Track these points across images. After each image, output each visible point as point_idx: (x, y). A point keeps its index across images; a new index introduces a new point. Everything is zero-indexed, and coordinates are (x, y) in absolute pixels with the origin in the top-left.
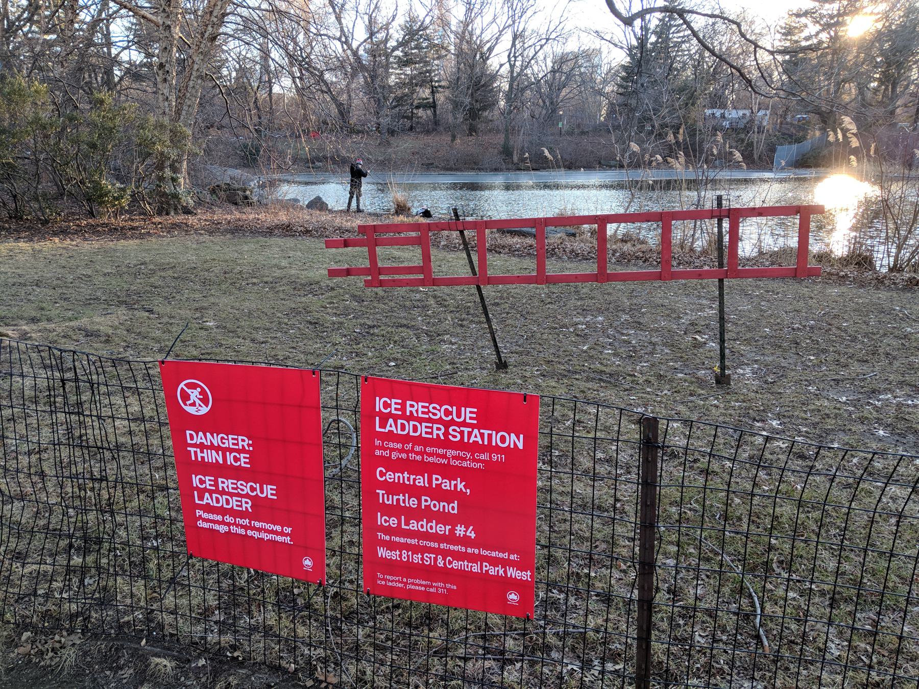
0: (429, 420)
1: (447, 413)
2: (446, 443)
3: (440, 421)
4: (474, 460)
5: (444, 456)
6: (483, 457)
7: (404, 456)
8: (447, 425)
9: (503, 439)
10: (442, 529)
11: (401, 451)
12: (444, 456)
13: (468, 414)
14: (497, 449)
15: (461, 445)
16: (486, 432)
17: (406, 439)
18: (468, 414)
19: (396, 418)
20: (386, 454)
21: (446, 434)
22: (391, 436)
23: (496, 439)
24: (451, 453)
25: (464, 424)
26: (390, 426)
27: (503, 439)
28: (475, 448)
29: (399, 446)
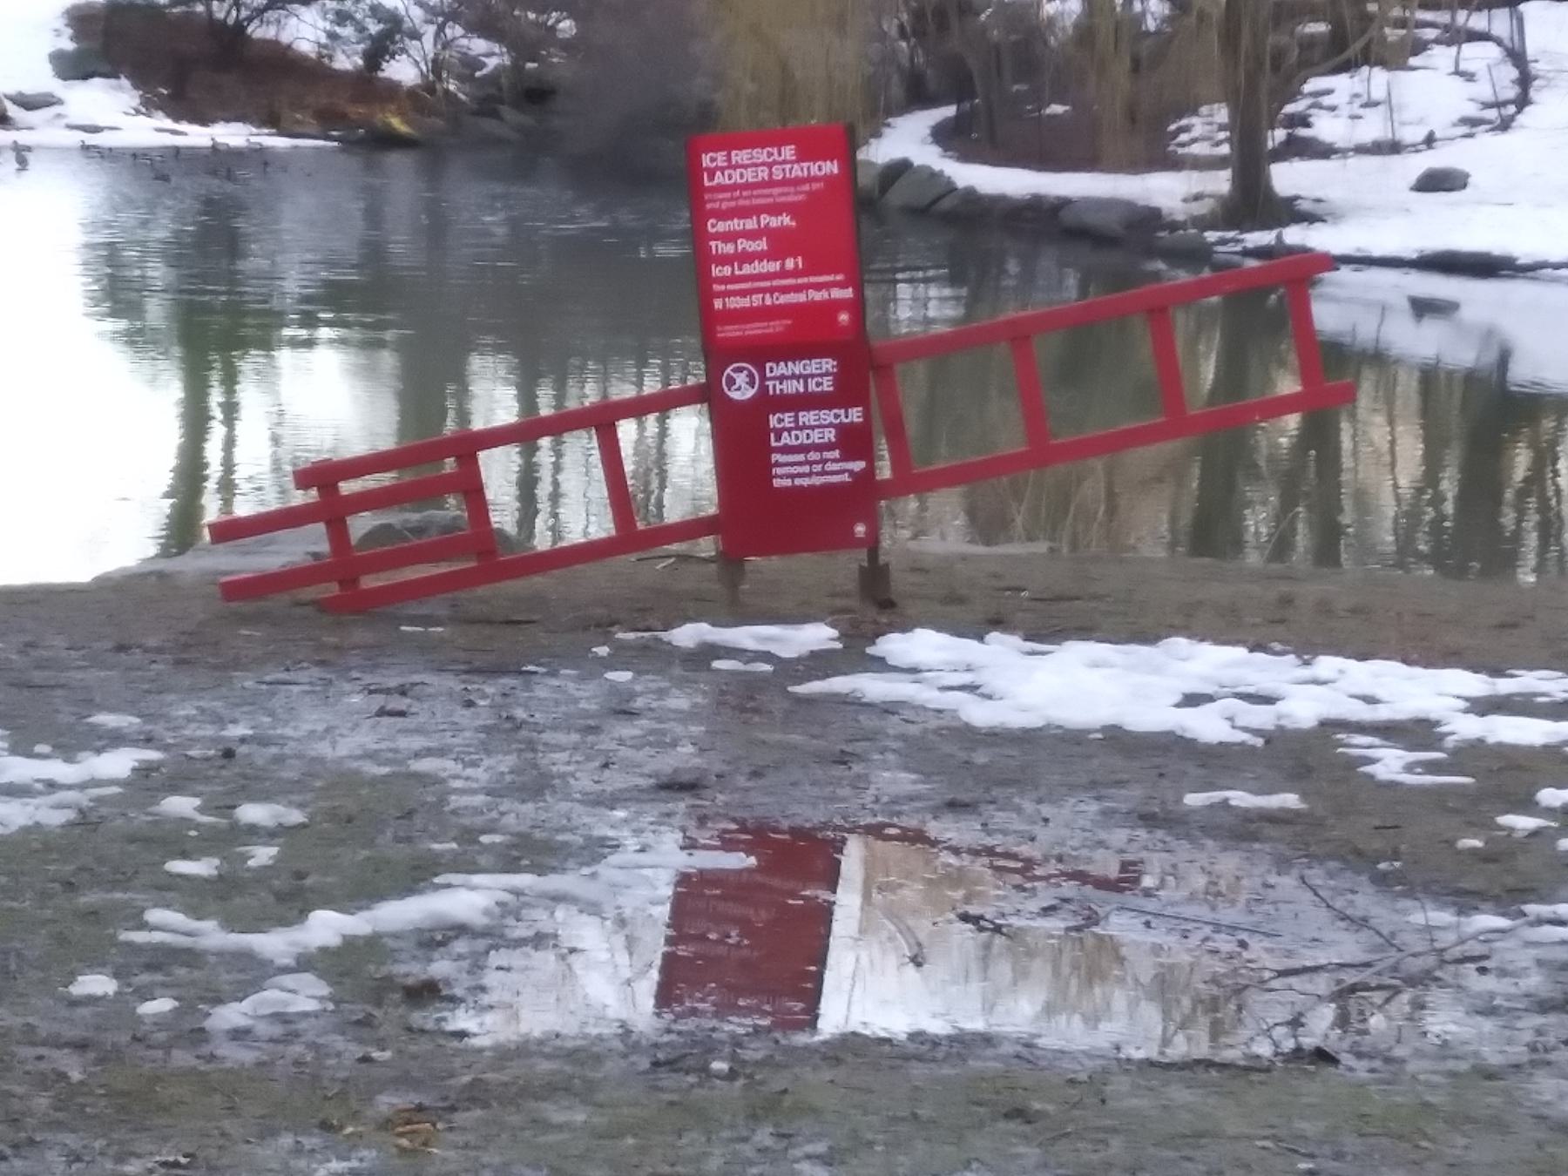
0: (756, 165)
1: (770, 155)
2: (771, 183)
3: (763, 164)
4: (796, 193)
5: (770, 196)
6: (806, 187)
7: (733, 204)
8: (770, 165)
9: (820, 168)
10: (774, 266)
11: (732, 199)
12: (770, 196)
13: (788, 152)
14: (816, 179)
15: (785, 182)
16: (805, 165)
17: (734, 187)
18: (788, 152)
19: (722, 170)
20: (716, 205)
21: (771, 174)
22: (722, 188)
23: (814, 170)
24: (776, 191)
25: (785, 162)
26: (719, 179)
27: (820, 168)
28: (797, 182)
29: (728, 195)
